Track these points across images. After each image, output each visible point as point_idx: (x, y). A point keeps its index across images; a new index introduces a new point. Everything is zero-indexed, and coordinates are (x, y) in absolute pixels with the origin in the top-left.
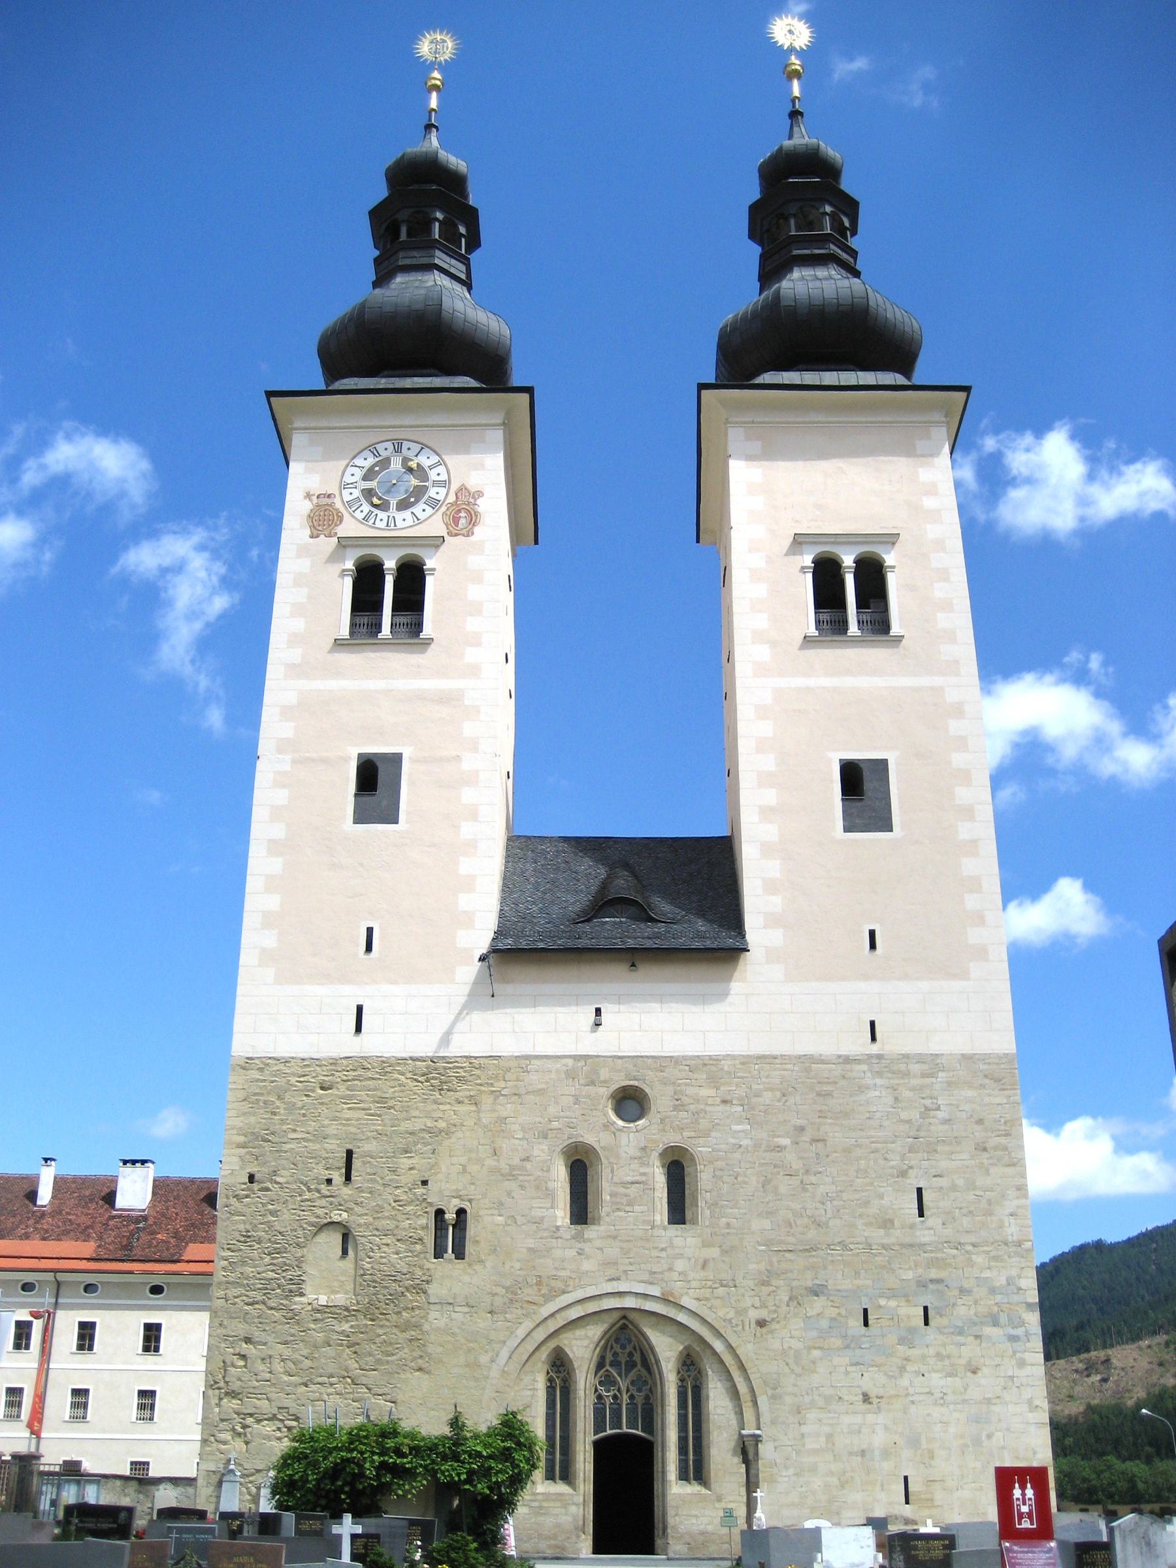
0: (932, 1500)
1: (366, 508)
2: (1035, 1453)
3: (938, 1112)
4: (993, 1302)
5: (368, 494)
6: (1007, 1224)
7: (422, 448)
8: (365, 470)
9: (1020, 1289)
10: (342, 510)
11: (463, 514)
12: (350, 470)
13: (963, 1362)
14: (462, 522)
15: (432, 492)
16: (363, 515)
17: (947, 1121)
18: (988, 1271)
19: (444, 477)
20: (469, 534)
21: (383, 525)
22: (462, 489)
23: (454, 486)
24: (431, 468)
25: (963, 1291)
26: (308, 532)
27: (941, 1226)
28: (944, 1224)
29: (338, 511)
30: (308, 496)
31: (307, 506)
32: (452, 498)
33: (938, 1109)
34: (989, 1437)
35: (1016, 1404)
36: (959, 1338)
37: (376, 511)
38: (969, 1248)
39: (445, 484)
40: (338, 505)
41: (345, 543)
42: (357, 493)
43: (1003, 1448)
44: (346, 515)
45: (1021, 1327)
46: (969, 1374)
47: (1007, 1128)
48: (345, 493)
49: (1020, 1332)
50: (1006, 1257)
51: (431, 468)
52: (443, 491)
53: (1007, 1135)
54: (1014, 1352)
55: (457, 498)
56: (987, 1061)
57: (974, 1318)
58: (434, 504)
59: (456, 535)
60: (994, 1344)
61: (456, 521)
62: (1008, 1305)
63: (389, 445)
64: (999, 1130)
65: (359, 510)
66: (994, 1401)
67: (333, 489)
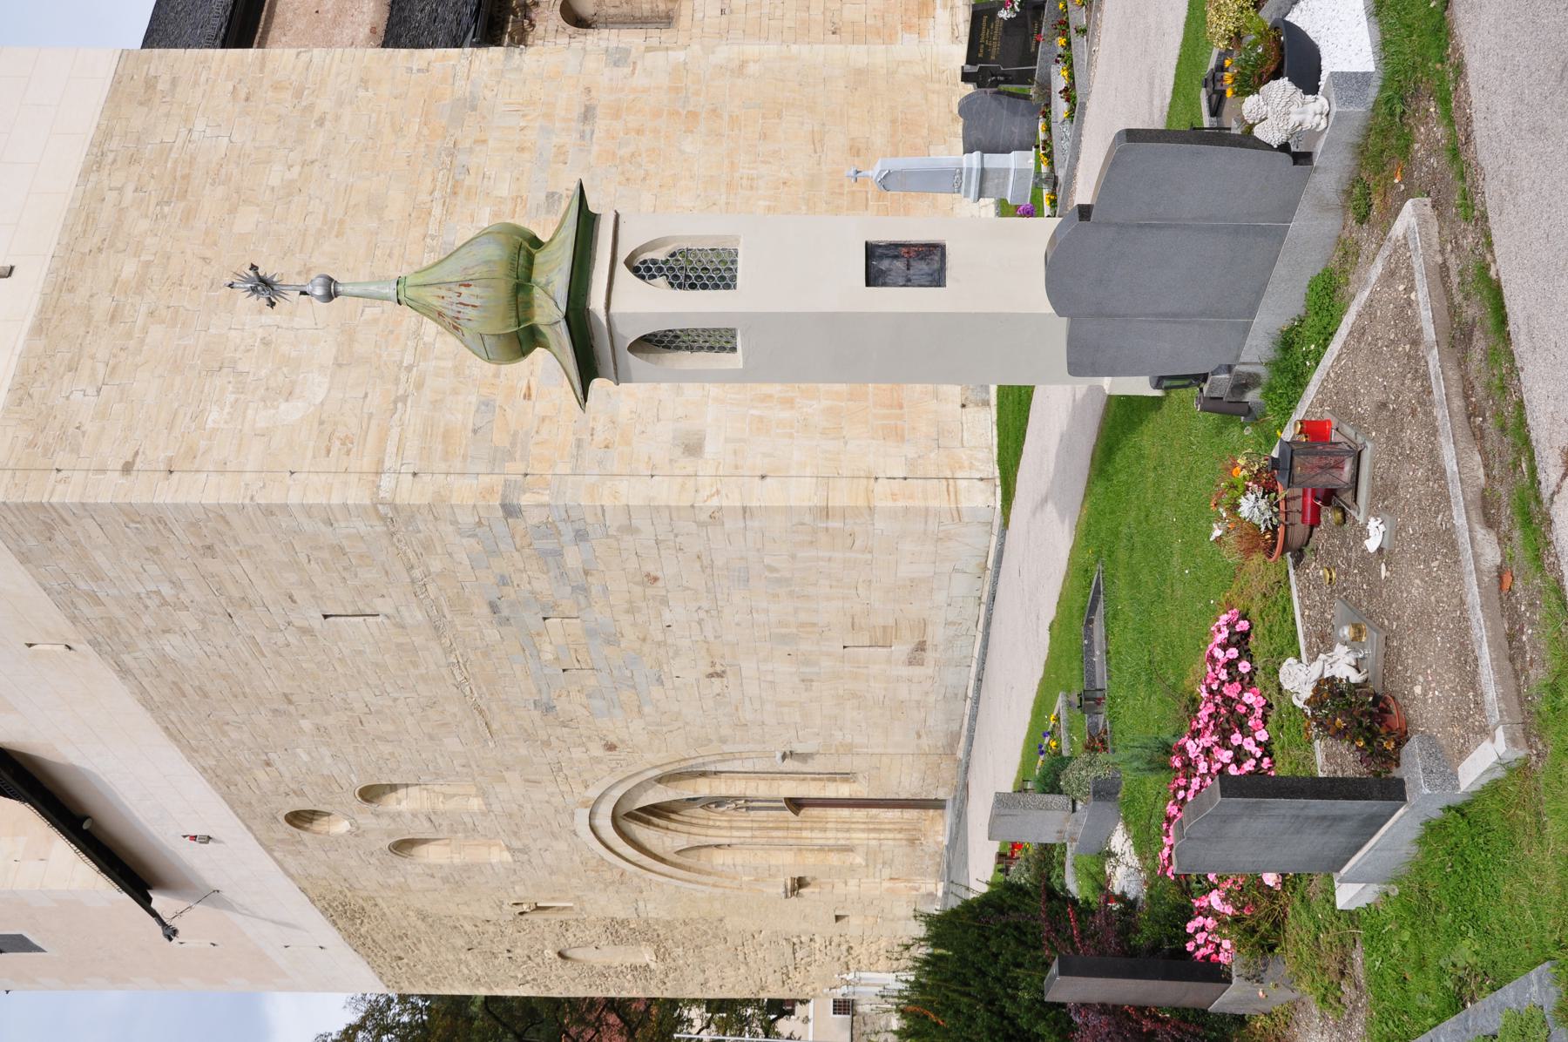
0: (885, 628)
2: (803, 524)
3: (163, 593)
4: (516, 555)
6: (353, 531)
9: (480, 524)
13: (638, 590)
17: (176, 584)
18: (455, 556)
25: (504, 581)
27: (387, 599)
28: (383, 596)
33: (158, 593)
34: (772, 569)
35: (709, 540)
36: (593, 592)
38: (417, 573)
43: (793, 557)
45: (557, 527)
46: (660, 584)
47: (147, 519)
49: (568, 531)
50: (421, 536)
53: (160, 520)
54: (608, 536)
56: (15, 536)
57: (551, 574)
60: (596, 558)
62: (517, 539)
64: (158, 530)
66: (706, 562)
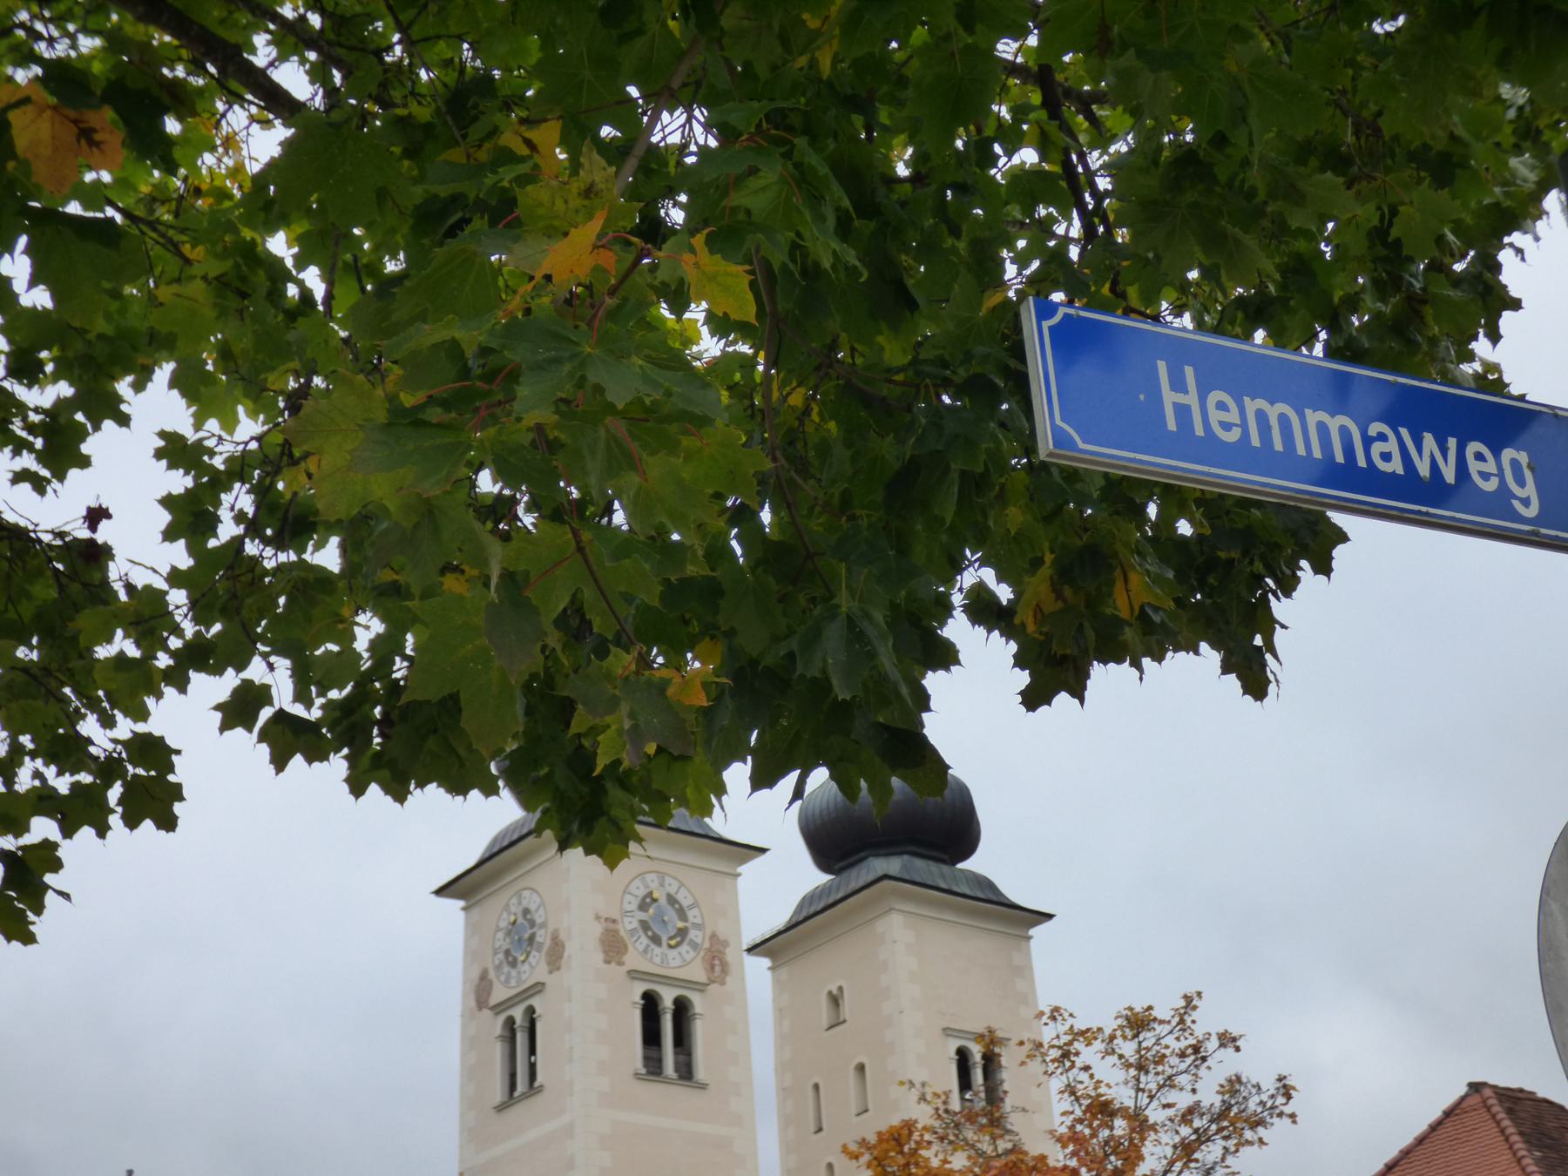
1: (644, 940)
5: (645, 926)
7: (680, 887)
8: (639, 899)
10: (626, 938)
11: (717, 962)
12: (628, 897)
14: (717, 969)
15: (693, 934)
16: (641, 948)
19: (698, 921)
20: (723, 983)
21: (657, 960)
22: (713, 936)
23: (708, 932)
24: (691, 907)
26: (600, 956)
29: (622, 938)
30: (598, 918)
31: (597, 929)
32: (707, 945)
37: (653, 946)
39: (698, 927)
40: (622, 933)
41: (635, 975)
42: (635, 924)
44: (630, 948)
48: (626, 920)
51: (691, 907)
52: (700, 934)
55: (711, 945)
58: (694, 946)
59: (713, 982)
61: (713, 967)
63: (653, 876)
65: (638, 943)
67: (616, 916)
